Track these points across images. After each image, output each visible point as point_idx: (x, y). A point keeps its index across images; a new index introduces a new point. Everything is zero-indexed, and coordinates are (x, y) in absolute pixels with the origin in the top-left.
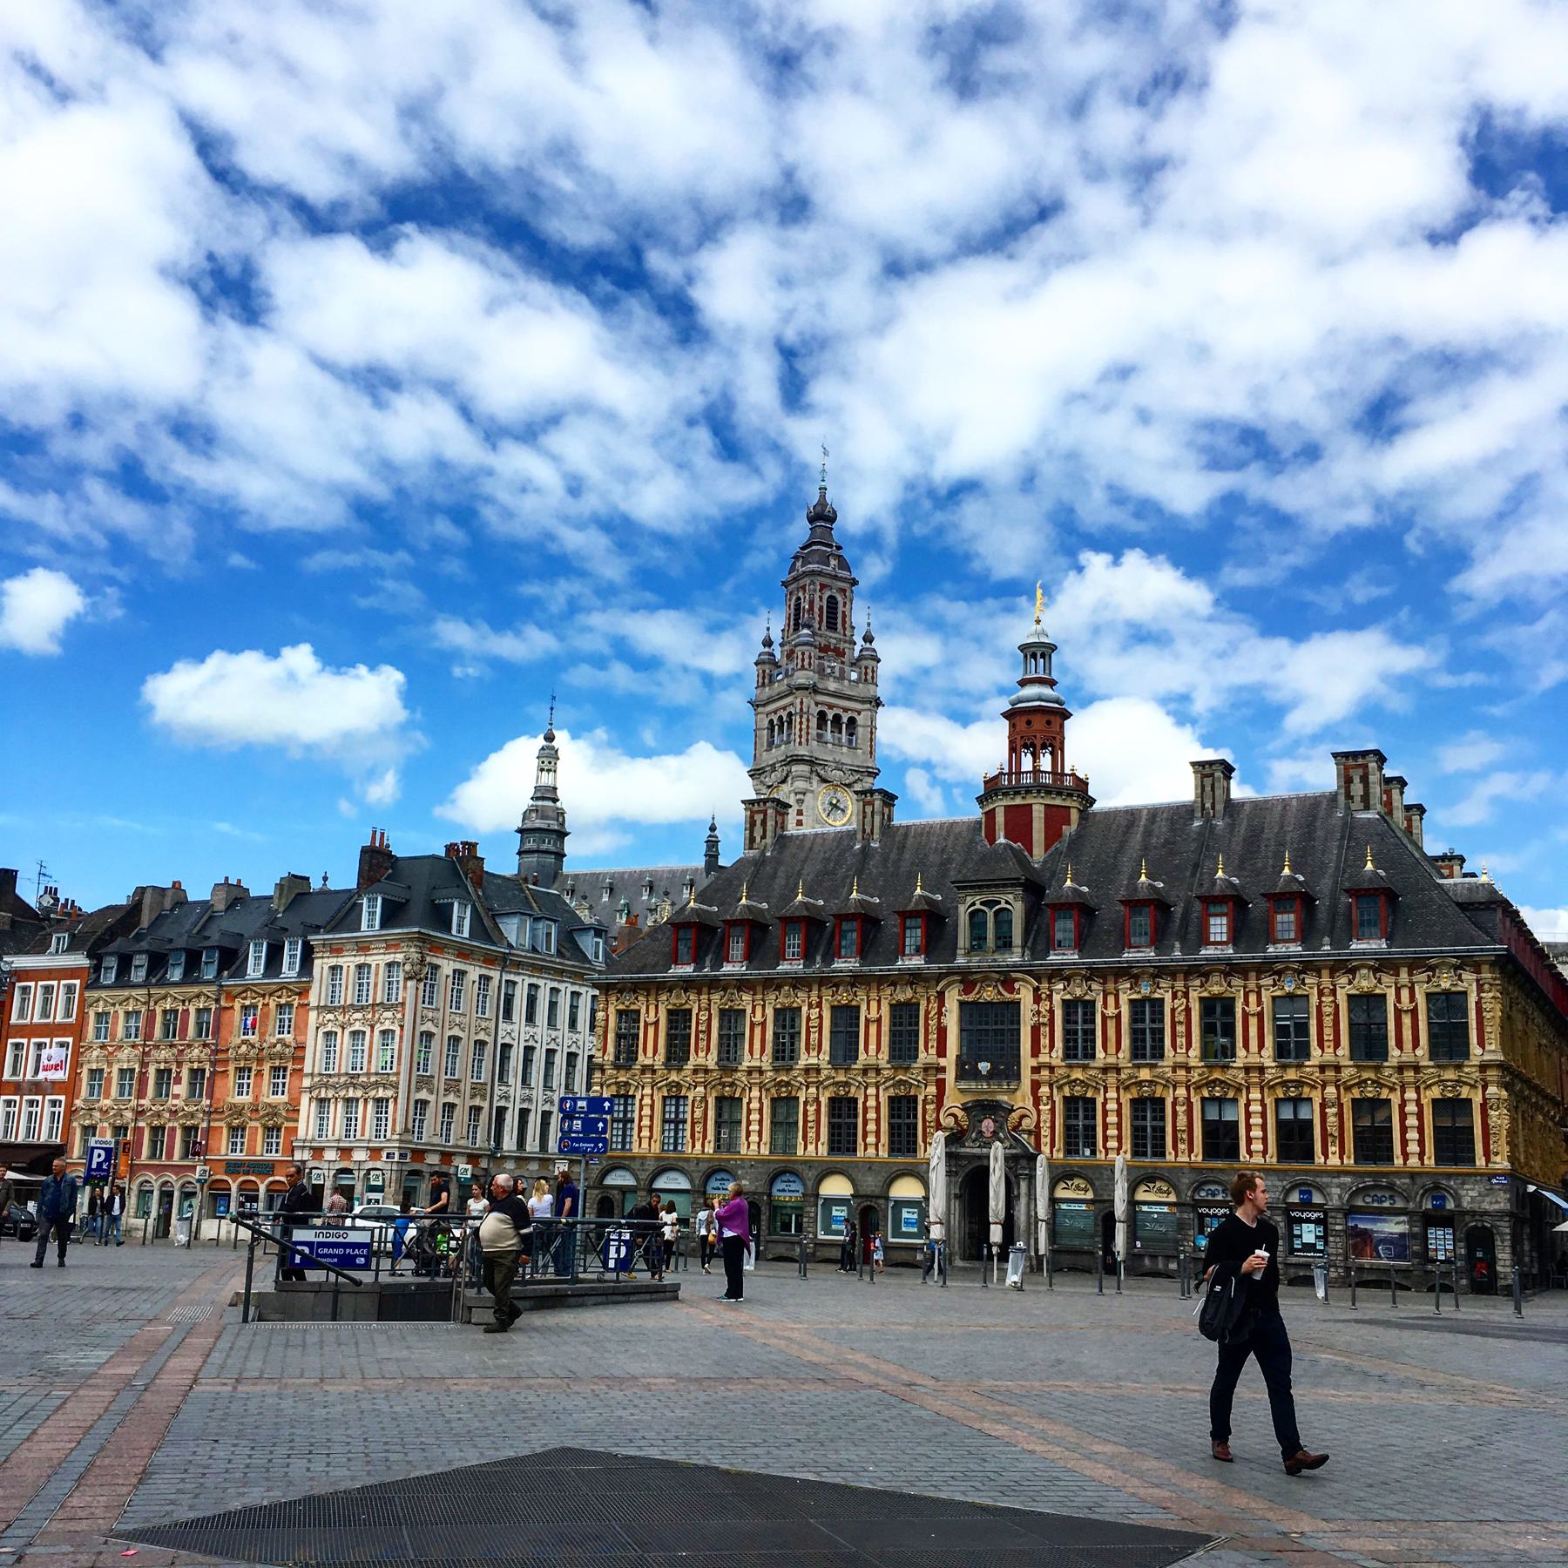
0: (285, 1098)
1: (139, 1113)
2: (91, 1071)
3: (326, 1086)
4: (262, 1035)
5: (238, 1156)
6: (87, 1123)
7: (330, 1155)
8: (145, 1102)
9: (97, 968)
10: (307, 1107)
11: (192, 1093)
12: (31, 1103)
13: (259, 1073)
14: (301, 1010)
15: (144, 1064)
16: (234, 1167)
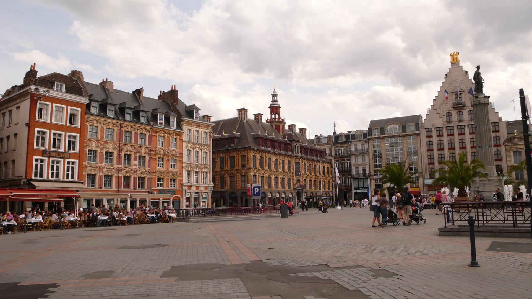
0: (177, 170)
1: (119, 170)
2: (90, 151)
3: (191, 167)
4: (168, 146)
5: (160, 188)
6: (93, 173)
7: (194, 188)
8: (122, 166)
9: (88, 106)
10: (185, 173)
11: (140, 165)
12: (53, 162)
13: (168, 160)
14: (181, 141)
15: (120, 151)
16: (160, 192)
